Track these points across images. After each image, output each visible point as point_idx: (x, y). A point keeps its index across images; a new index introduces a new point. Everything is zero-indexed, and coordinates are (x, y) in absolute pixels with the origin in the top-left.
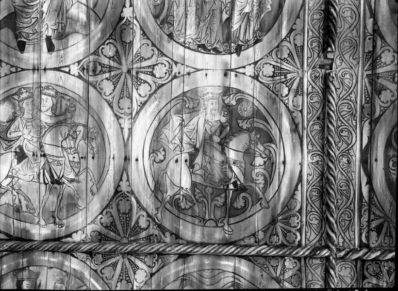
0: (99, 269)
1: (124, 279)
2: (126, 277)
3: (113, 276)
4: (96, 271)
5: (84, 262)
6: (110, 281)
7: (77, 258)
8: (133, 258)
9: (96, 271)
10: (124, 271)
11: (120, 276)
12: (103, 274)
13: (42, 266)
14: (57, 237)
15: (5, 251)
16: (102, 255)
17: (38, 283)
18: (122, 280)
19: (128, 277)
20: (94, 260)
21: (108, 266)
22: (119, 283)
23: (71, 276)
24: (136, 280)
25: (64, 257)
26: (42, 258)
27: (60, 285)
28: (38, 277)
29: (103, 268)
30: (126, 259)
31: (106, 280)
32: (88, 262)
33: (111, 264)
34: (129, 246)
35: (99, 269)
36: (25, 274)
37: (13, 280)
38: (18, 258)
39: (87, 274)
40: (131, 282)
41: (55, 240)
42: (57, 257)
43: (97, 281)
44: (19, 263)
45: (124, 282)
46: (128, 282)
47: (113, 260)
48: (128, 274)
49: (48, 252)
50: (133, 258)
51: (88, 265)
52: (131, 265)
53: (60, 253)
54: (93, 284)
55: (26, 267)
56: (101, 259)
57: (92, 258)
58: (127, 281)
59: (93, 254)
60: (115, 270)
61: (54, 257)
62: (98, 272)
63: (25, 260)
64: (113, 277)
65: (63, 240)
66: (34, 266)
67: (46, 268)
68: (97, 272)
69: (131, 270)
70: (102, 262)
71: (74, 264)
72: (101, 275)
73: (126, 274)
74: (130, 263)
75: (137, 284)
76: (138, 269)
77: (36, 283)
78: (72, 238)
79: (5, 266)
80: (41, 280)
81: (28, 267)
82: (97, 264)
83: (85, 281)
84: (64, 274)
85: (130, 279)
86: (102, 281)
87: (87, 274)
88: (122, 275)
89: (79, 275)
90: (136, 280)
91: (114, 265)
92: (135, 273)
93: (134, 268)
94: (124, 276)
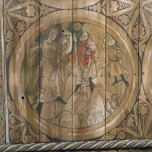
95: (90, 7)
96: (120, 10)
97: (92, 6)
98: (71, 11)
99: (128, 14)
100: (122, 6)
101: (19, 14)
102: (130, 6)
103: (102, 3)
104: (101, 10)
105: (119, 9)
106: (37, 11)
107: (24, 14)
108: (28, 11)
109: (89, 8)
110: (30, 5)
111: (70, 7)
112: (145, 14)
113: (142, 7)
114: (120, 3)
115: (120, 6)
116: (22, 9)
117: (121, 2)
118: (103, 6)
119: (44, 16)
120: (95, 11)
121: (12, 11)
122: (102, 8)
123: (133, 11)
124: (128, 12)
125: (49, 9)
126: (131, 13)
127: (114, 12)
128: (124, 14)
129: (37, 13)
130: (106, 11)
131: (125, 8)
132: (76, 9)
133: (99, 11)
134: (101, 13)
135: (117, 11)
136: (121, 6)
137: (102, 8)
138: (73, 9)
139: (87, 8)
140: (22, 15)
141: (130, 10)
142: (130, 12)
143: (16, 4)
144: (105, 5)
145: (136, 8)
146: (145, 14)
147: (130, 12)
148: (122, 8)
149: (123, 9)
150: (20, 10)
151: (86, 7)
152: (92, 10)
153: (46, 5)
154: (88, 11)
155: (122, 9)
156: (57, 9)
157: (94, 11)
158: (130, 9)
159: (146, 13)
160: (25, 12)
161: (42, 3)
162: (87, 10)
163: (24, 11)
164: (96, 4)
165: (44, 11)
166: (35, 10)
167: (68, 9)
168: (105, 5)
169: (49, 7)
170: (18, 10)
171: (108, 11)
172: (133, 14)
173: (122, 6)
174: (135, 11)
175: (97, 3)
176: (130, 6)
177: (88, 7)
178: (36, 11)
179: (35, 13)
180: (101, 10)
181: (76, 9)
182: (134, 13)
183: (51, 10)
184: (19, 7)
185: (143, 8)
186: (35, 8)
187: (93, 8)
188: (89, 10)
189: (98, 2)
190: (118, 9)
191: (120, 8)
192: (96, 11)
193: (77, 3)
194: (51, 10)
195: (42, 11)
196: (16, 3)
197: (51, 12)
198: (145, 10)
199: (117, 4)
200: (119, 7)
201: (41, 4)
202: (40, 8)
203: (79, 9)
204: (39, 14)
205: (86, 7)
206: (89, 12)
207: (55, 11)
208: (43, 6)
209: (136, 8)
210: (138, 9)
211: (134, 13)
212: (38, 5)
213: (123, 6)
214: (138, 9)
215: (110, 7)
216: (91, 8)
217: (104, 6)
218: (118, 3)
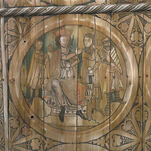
0: (117, 24)
1: (136, 30)
2: (137, 29)
3: (128, 29)
4: (115, 26)
5: (105, 20)
6: (125, 33)
7: (100, 18)
8: (142, 15)
9: (115, 26)
10: (136, 25)
11: (133, 28)
12: (120, 28)
13: (74, 25)
14: (84, 3)
15: (46, 15)
16: (119, 14)
17: (72, 37)
18: (135, 31)
19: (139, 29)
20: (113, 18)
21: (123, 22)
22: (133, 34)
23: (96, 31)
24: (145, 31)
25: (90, 18)
26: (74, 19)
27: (88, 38)
28: (71, 33)
29: (120, 24)
30: (137, 16)
31: (122, 33)
32: (109, 20)
33: (126, 20)
34: (140, 4)
35: (117, 24)
36: (62, 32)
37: (53, 37)
38: (56, 20)
39: (108, 29)
40: (141, 33)
41: (82, 5)
42: (85, 18)
43: (116, 34)
44: (56, 24)
45: (136, 33)
46: (139, 33)
47: (127, 17)
48: (139, 27)
49: (78, 14)
50: (142, 15)
51: (108, 22)
52: (141, 21)
53: (87, 15)
54: (113, 36)
55: (62, 26)
56: (118, 17)
57: (111, 17)
58: (138, 32)
59: (112, 14)
60: (129, 25)
61: (83, 18)
62: (116, 27)
63: (61, 21)
64: (128, 30)
65: (89, 4)
66: (68, 25)
67: (77, 26)
68: (116, 28)
69: (141, 23)
70: (119, 20)
71: (98, 22)
72: (120, 29)
73: (137, 27)
74: (139, 18)
75: (146, 34)
76: (146, 23)
77: (70, 37)
78: (96, 3)
79: (46, 26)
80: (74, 35)
81: (64, 26)
82: (115, 21)
83: (107, 34)
84: (91, 30)
85: (140, 30)
86: (120, 34)
87: (108, 29)
88: (134, 27)
89: (102, 31)
90: (145, 31)
91: (128, 21)
92: (144, 26)
93: (143, 23)
94: (136, 29)
95: (93, 141)
96: (124, 144)
97: (96, 140)
98: (75, 145)
99: (131, 148)
100: (126, 141)
101: (24, 147)
102: (133, 141)
103: (105, 138)
104: (105, 144)
105: (122, 144)
106: (42, 145)
107: (29, 147)
108: (33, 144)
109: (93, 143)
110: (35, 139)
111: (75, 141)
112: (148, 148)
113: (145, 141)
114: (123, 138)
115: (123, 140)
116: (27, 142)
117: (125, 137)
118: (107, 140)
119: (48, 150)
120: (99, 145)
121: (17, 144)
122: (106, 142)
123: (136, 146)
124: (132, 147)
125: (53, 142)
126: (135, 148)
127: (117, 146)
128: (128, 149)
129: (42, 146)
130: (109, 145)
131: (129, 143)
132: (80, 143)
133: (103, 145)
134: (105, 147)
135: (121, 145)
136: (125, 140)
137: (106, 142)
138: (77, 143)
139: (91, 142)
140: (27, 148)
141: (133, 145)
142: (133, 147)
143: (21, 138)
144: (109, 139)
145: (139, 143)
146: (148, 148)
147: (133, 147)
148: (125, 142)
149: (126, 144)
150: (25, 143)
151: (90, 141)
152: (96, 144)
153: (50, 139)
154: (92, 145)
155: (125, 144)
156: (61, 142)
157: (98, 145)
158: (133, 144)
159: (149, 147)
160: (30, 145)
161: (47, 137)
162: (91, 144)
163: (29, 144)
164: (100, 138)
165: (48, 145)
166: (40, 143)
167: (73, 143)
168: (109, 139)
169: (54, 141)
170: (23, 144)
171: (111, 146)
172: (136, 149)
173: (126, 141)
174: (138, 146)
175: (101, 137)
176: (133, 141)
177: (92, 141)
178: (40, 144)
179: (40, 147)
180: (105, 144)
181: (80, 143)
182: (137, 148)
183: (55, 143)
184: (24, 140)
185: (146, 143)
186: (39, 142)
187: (97, 142)
188: (92, 144)
189: (102, 137)
190: (122, 144)
191: (124, 143)
192: (100, 146)
193: (81, 137)
194: (55, 143)
195: (47, 145)
196: (21, 136)
197: (55, 146)
198: (148, 145)
199: (121, 138)
200: (122, 142)
201: (45, 138)
202: (45, 142)
203: (83, 143)
204: (43, 147)
205: (90, 141)
206: (93, 146)
207: (60, 144)
208: (47, 139)
209: (139, 143)
210: (141, 144)
211: (137, 148)
212: (43, 138)
213: (127, 140)
214: (141, 144)
215: (114, 141)
216: (95, 142)
217: (108, 140)
218: (121, 138)
